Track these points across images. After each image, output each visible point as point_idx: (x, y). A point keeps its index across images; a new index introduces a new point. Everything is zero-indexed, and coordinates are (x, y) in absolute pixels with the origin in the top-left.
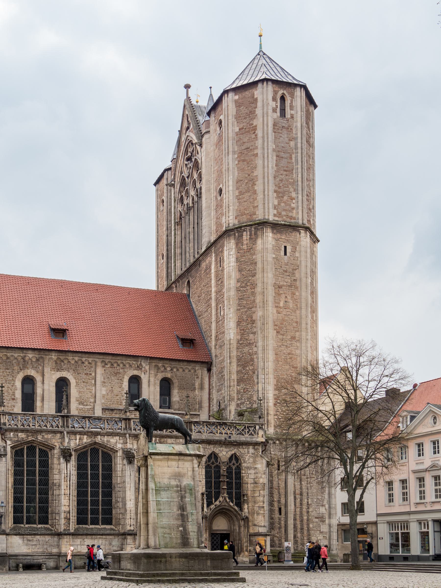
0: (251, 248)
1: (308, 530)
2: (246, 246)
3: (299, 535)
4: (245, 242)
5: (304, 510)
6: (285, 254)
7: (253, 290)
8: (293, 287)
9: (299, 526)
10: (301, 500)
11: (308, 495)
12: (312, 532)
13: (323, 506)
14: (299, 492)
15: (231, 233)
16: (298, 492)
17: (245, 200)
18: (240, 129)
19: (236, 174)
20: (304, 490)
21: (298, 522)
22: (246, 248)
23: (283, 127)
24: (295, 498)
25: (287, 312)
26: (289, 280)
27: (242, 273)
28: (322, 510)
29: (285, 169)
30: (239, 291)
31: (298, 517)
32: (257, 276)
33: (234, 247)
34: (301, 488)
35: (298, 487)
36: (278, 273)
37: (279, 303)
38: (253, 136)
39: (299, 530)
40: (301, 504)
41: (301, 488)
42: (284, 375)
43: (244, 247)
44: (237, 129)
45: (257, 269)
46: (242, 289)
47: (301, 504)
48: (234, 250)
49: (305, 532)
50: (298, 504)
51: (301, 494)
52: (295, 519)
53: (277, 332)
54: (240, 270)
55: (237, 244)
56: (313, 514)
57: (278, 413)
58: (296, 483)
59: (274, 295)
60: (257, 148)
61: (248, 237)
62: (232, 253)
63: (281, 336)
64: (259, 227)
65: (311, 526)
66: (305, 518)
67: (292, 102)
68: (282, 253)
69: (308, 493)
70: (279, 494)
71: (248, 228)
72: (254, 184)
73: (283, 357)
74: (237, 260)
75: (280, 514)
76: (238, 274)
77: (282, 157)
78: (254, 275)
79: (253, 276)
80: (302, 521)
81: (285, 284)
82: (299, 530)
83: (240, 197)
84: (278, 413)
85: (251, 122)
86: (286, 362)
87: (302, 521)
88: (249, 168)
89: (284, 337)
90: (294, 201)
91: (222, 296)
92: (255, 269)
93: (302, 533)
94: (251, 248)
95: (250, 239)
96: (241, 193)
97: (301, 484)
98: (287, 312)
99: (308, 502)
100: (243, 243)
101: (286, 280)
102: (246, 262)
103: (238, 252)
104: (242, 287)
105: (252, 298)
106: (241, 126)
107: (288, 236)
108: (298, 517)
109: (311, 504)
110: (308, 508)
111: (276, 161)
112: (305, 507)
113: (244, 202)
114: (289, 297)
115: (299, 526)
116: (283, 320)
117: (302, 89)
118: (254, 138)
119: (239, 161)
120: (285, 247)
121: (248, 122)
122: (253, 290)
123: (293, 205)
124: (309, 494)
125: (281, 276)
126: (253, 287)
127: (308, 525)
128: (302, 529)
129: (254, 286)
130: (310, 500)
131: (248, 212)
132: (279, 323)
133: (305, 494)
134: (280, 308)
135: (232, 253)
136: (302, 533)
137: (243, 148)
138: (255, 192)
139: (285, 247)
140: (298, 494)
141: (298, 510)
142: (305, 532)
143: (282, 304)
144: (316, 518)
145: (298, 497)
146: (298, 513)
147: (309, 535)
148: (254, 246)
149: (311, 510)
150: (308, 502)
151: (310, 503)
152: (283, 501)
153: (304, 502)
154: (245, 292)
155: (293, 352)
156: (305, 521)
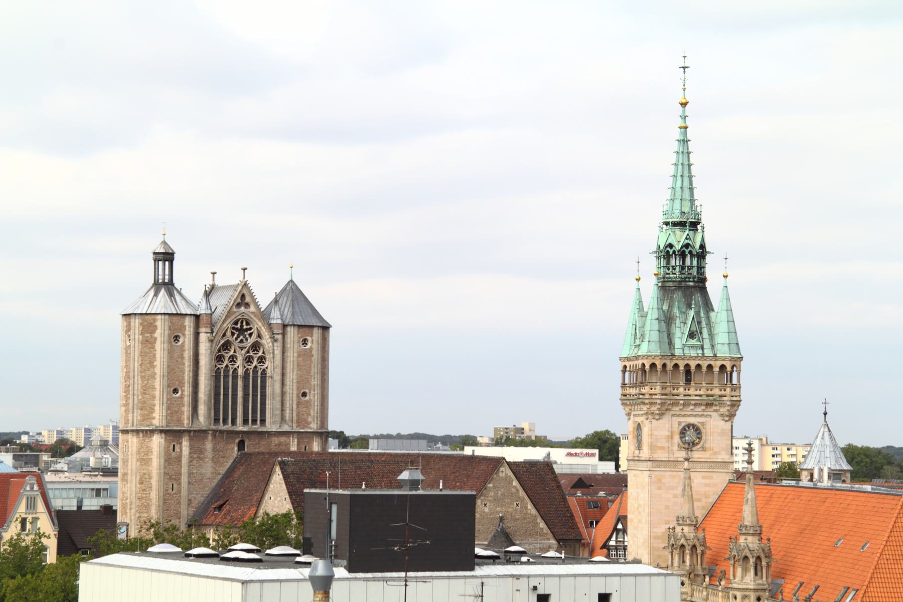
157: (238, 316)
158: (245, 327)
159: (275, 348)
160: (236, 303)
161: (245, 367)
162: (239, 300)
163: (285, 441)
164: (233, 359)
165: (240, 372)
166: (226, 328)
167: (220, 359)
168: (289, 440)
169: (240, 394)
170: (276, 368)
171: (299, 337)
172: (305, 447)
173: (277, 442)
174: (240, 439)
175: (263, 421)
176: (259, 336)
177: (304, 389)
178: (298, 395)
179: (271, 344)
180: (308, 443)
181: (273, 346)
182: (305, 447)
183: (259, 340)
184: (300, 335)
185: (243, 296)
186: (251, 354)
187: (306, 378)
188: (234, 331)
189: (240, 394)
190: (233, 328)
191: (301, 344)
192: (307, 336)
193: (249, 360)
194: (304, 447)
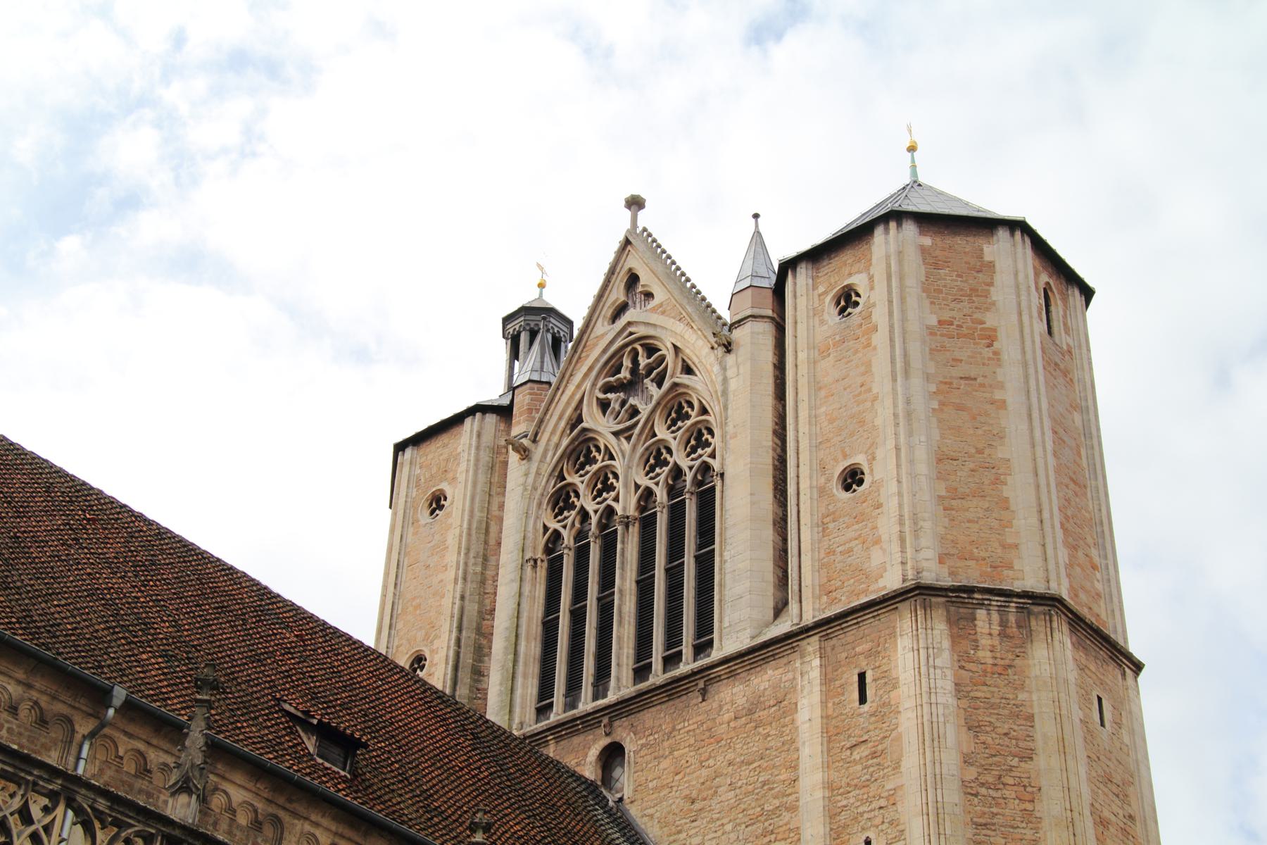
0: (1010, 666)
2: (989, 654)
4: (985, 642)
6: (1102, 724)
7: (1029, 806)
8: (1130, 837)
15: (934, 600)
17: (970, 515)
18: (940, 322)
19: (936, 434)
22: (990, 661)
23: (1056, 364)
26: (1121, 813)
27: (983, 738)
29: (1071, 474)
30: (976, 795)
32: (1041, 761)
33: (946, 644)
36: (1094, 774)
38: (987, 353)
43: (980, 654)
44: (933, 321)
45: (1038, 736)
46: (983, 791)
48: (946, 655)
54: (974, 727)
55: (955, 640)
60: (1001, 386)
61: (996, 629)
62: (938, 662)
64: (1036, 609)
67: (1065, 316)
71: (996, 601)
72: (998, 481)
74: (958, 691)
76: (966, 736)
77: (1064, 442)
78: (1028, 756)
79: (1022, 759)
81: (1113, 818)
83: (954, 503)
85: (977, 316)
88: (980, 432)
90: (1098, 575)
91: (883, 802)
92: (1030, 737)
94: (1010, 666)
95: (1003, 635)
96: (954, 493)
100: (976, 641)
102: (992, 706)
103: (962, 667)
104: (982, 785)
105: (1029, 834)
106: (946, 316)
107: (1101, 670)
113: (969, 521)
117: (1083, 298)
118: (989, 359)
119: (942, 404)
120: (1100, 699)
121: (966, 311)
122: (1029, 806)
125: (1101, 786)
126: (1028, 797)
129: (1029, 792)
131: (983, 554)
135: (938, 662)
137: (957, 372)
138: (1004, 504)
139: (1100, 699)
148: (1018, 662)
154: (997, 805)
157: (612, 342)
158: (643, 361)
159: (730, 373)
160: (608, 311)
161: (637, 487)
162: (617, 294)
163: (776, 687)
164: (603, 484)
165: (627, 504)
166: (578, 397)
167: (562, 500)
168: (790, 675)
169: (626, 580)
170: (733, 437)
171: (819, 295)
172: (862, 677)
173: (741, 701)
174: (605, 741)
175: (702, 648)
176: (688, 370)
177: (845, 456)
178: (822, 491)
179: (716, 368)
180: (871, 654)
181: (724, 369)
182: (862, 677)
183: (685, 379)
184: (821, 289)
185: (633, 279)
186: (662, 433)
187: (852, 417)
188: (609, 396)
189: (626, 580)
190: (608, 388)
191: (831, 313)
192: (850, 275)
193: (656, 457)
194: (856, 678)
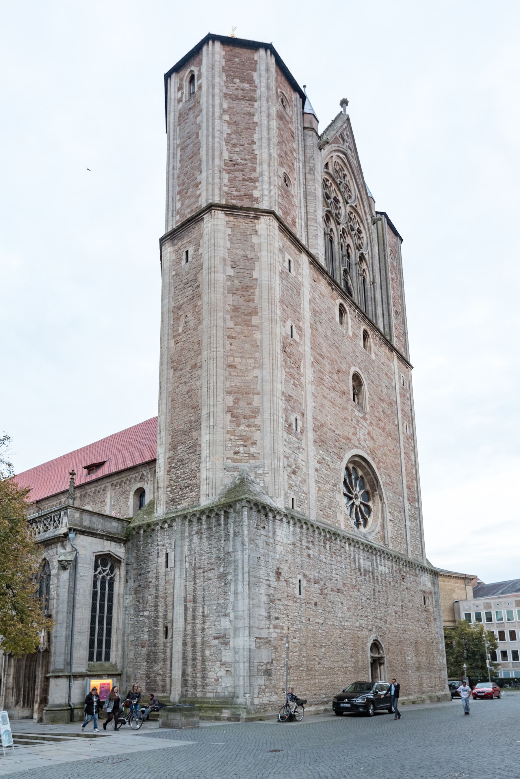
1: (203, 661)
3: (189, 670)
5: (198, 626)
9: (190, 655)
10: (194, 610)
11: (204, 601)
12: (208, 664)
13: (226, 615)
14: (192, 597)
16: (190, 597)
20: (199, 593)
21: (189, 649)
24: (186, 609)
25: (187, 335)
28: (225, 623)
31: (189, 640)
34: (194, 591)
35: (190, 588)
37: (178, 330)
39: (190, 662)
40: (194, 617)
41: (194, 591)
42: (181, 425)
47: (194, 617)
49: (199, 665)
50: (189, 618)
51: (195, 601)
52: (185, 644)
53: (175, 370)
56: (211, 631)
57: (172, 482)
58: (188, 584)
59: (172, 323)
63: (180, 372)
65: (207, 653)
66: (199, 639)
68: (184, 262)
69: (204, 597)
70: (166, 605)
73: (181, 400)
75: (166, 638)
80: (194, 646)
82: (190, 662)
84: (172, 482)
86: (185, 405)
87: (194, 646)
89: (183, 371)
93: (194, 666)
97: (195, 583)
98: (187, 335)
99: (203, 612)
101: (187, 294)
108: (189, 640)
109: (208, 616)
110: (204, 623)
111: (181, 155)
112: (199, 621)
114: (189, 315)
115: (190, 655)
116: (182, 349)
123: (198, 193)
124: (206, 599)
127: (203, 651)
128: (194, 659)
130: (206, 609)
132: (177, 356)
133: (200, 600)
134: (179, 335)
136: (194, 666)
140: (190, 602)
141: (189, 627)
142: (199, 665)
143: (181, 330)
144: (216, 638)
145: (190, 605)
146: (189, 632)
147: (204, 669)
149: (207, 625)
150: (203, 612)
151: (206, 613)
152: (170, 615)
153: (198, 614)
155: (194, 387)
156: (199, 645)
